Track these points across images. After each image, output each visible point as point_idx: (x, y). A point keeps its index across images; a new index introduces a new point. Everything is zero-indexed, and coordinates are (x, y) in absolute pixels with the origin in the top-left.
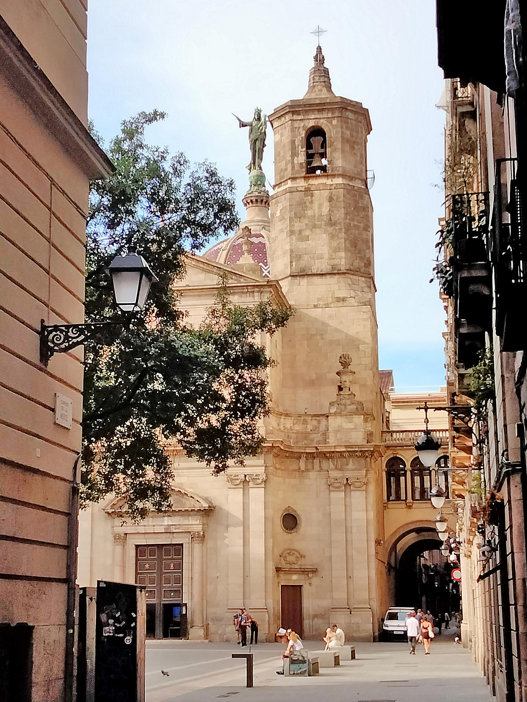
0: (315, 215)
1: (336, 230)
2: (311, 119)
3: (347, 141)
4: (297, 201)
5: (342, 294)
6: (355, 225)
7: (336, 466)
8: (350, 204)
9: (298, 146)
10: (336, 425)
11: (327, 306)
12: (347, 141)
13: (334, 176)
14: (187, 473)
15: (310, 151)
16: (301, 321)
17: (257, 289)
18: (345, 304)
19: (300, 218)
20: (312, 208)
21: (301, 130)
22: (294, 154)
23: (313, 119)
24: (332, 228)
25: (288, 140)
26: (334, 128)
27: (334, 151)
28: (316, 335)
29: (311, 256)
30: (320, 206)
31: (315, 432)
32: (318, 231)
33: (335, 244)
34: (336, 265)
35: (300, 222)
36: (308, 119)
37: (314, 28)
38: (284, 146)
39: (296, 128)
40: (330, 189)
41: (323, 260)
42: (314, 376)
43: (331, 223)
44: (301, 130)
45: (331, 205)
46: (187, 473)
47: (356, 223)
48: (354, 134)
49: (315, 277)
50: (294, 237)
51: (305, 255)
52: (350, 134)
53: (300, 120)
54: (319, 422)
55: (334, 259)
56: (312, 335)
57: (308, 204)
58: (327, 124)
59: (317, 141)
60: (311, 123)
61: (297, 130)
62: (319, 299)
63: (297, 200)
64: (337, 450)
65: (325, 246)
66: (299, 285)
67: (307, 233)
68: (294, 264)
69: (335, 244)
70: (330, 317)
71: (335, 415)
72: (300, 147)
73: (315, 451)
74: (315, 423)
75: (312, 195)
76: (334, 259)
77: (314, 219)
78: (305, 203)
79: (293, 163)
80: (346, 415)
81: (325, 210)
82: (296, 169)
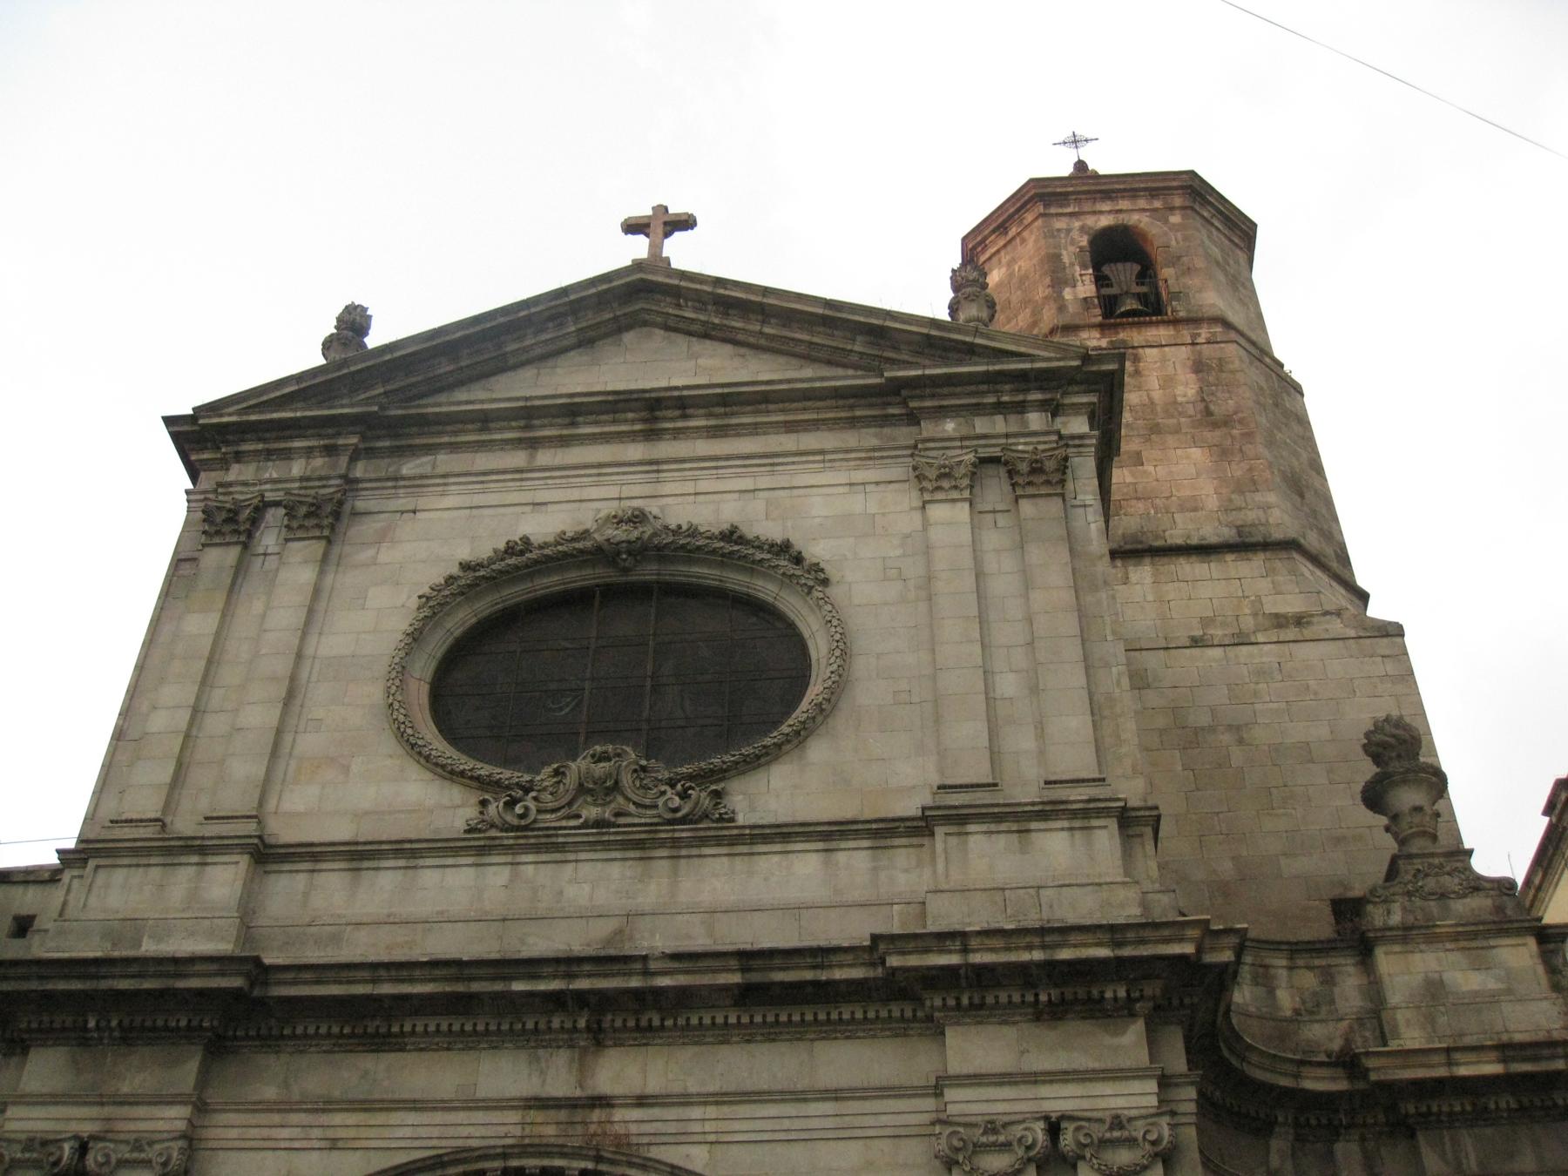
0: (1152, 403)
2: (1101, 212)
5: (1292, 604)
7: (1460, 1164)
9: (1072, 265)
10: (1417, 979)
11: (1241, 640)
13: (1194, 321)
14: (708, 1127)
15: (1106, 291)
16: (1148, 687)
17: (1036, 396)
18: (1308, 633)
20: (1139, 388)
21: (1075, 234)
22: (1059, 279)
23: (1110, 212)
24: (1218, 433)
25: (1035, 261)
26: (1177, 231)
27: (1183, 274)
28: (1212, 729)
30: (1168, 382)
31: (1318, 1017)
32: (1171, 440)
33: (1237, 470)
34: (1253, 525)
36: (1094, 213)
37: (1066, 134)
38: (1023, 279)
39: (1059, 230)
40: (1193, 344)
41: (1199, 514)
42: (1226, 868)
43: (1208, 418)
44: (1075, 234)
45: (1199, 380)
46: (708, 1127)
47: (1288, 441)
48: (1231, 262)
49: (1182, 560)
51: (1134, 502)
52: (1223, 257)
53: (1071, 215)
54: (1328, 978)
55: (1240, 509)
56: (1197, 731)
59: (1122, 275)
60: (1105, 221)
61: (1062, 235)
62: (1206, 622)
64: (1463, 1071)
65: (1204, 476)
69: (1237, 470)
70: (1261, 673)
71: (1405, 940)
72: (1077, 268)
73: (1342, 1085)
74: (1309, 980)
76: (1240, 509)
77: (1153, 411)
79: (1060, 297)
80: (1455, 937)
81: (1187, 388)
82: (1071, 310)
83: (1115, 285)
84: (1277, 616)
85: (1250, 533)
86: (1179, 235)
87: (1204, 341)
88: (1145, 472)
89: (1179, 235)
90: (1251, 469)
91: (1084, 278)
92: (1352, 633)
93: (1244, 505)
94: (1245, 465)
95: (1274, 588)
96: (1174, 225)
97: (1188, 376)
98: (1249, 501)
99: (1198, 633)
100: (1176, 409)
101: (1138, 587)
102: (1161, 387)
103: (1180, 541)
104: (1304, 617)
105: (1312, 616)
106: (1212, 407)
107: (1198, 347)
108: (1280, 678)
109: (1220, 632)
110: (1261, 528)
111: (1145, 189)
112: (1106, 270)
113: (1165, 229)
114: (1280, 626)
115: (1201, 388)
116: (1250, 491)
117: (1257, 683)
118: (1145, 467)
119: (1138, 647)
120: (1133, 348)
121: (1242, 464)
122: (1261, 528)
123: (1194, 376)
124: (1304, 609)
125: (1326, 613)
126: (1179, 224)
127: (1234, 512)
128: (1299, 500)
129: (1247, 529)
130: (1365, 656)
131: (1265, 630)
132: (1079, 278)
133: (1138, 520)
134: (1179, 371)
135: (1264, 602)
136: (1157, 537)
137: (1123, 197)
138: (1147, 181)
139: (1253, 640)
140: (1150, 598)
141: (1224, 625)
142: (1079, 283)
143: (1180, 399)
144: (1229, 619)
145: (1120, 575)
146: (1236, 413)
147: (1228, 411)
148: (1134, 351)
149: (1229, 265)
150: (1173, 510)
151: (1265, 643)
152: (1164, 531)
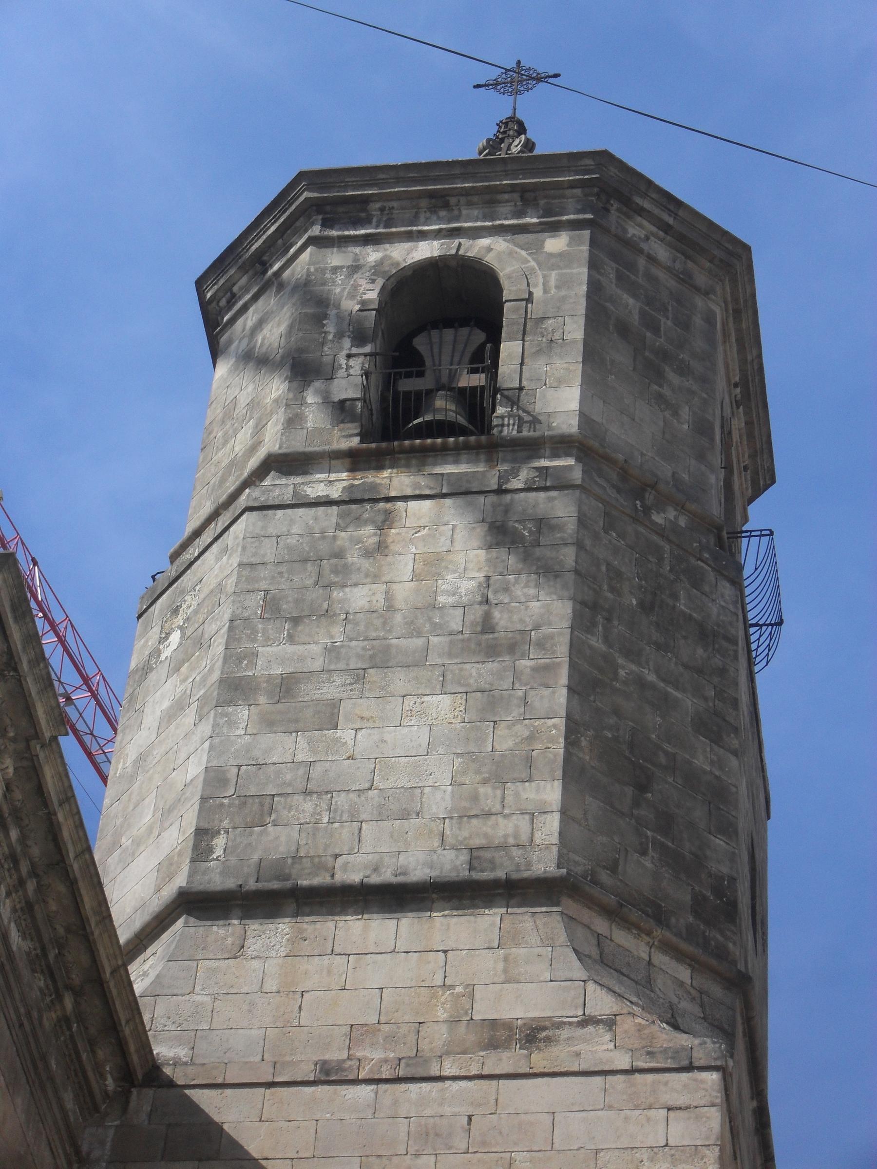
0: (390, 607)
1: (517, 675)
3: (623, 330)
4: (289, 548)
6: (642, 684)
8: (616, 575)
12: (623, 330)
15: (407, 385)
18: (540, 1060)
19: (296, 621)
20: (375, 578)
29: (341, 800)
34: (503, 847)
35: (291, 639)
47: (651, 677)
48: (666, 323)
50: (243, 713)
52: (643, 314)
55: (489, 814)
57: (354, 557)
58: (511, 254)
63: (292, 541)
66: (239, 951)
67: (330, 691)
68: (220, 843)
75: (386, 522)
76: (489, 814)
78: (339, 554)
83: (428, 373)
84: (493, 1024)
85: (492, 861)
86: (553, 276)
87: (520, 486)
88: (336, 740)
89: (553, 276)
90: (531, 738)
91: (352, 362)
92: (623, 1061)
93: (497, 808)
94: (522, 730)
95: (505, 971)
96: (551, 255)
97: (472, 554)
98: (509, 800)
99: (336, 1054)
100: (430, 619)
101: (255, 964)
102: (416, 577)
103: (355, 878)
104: (544, 1029)
105: (560, 1025)
106: (497, 614)
107: (508, 497)
108: (463, 1146)
109: (377, 1055)
110: (516, 852)
111: (513, 188)
112: (420, 343)
113: (533, 263)
114: (493, 1045)
115: (488, 578)
116: (514, 781)
117: (417, 1155)
118: (339, 733)
119: (220, 1080)
120: (388, 499)
121: (518, 727)
122: (516, 852)
123: (482, 553)
124: (548, 1014)
125: (587, 1021)
126: (561, 255)
127: (474, 821)
128: (629, 791)
129: (487, 855)
130: (636, 1108)
131: (464, 1052)
132: (343, 362)
133: (296, 835)
134: (458, 546)
135: (477, 995)
136: (320, 867)
137: (470, 204)
138: (514, 175)
139: (434, 1071)
140: (271, 985)
141: (391, 1039)
142: (342, 373)
143: (442, 599)
144: (404, 1029)
145: (230, 940)
146: (537, 628)
147: (521, 621)
148: (389, 505)
149: (656, 330)
150: (363, 817)
151: (455, 1078)
152: (336, 856)
